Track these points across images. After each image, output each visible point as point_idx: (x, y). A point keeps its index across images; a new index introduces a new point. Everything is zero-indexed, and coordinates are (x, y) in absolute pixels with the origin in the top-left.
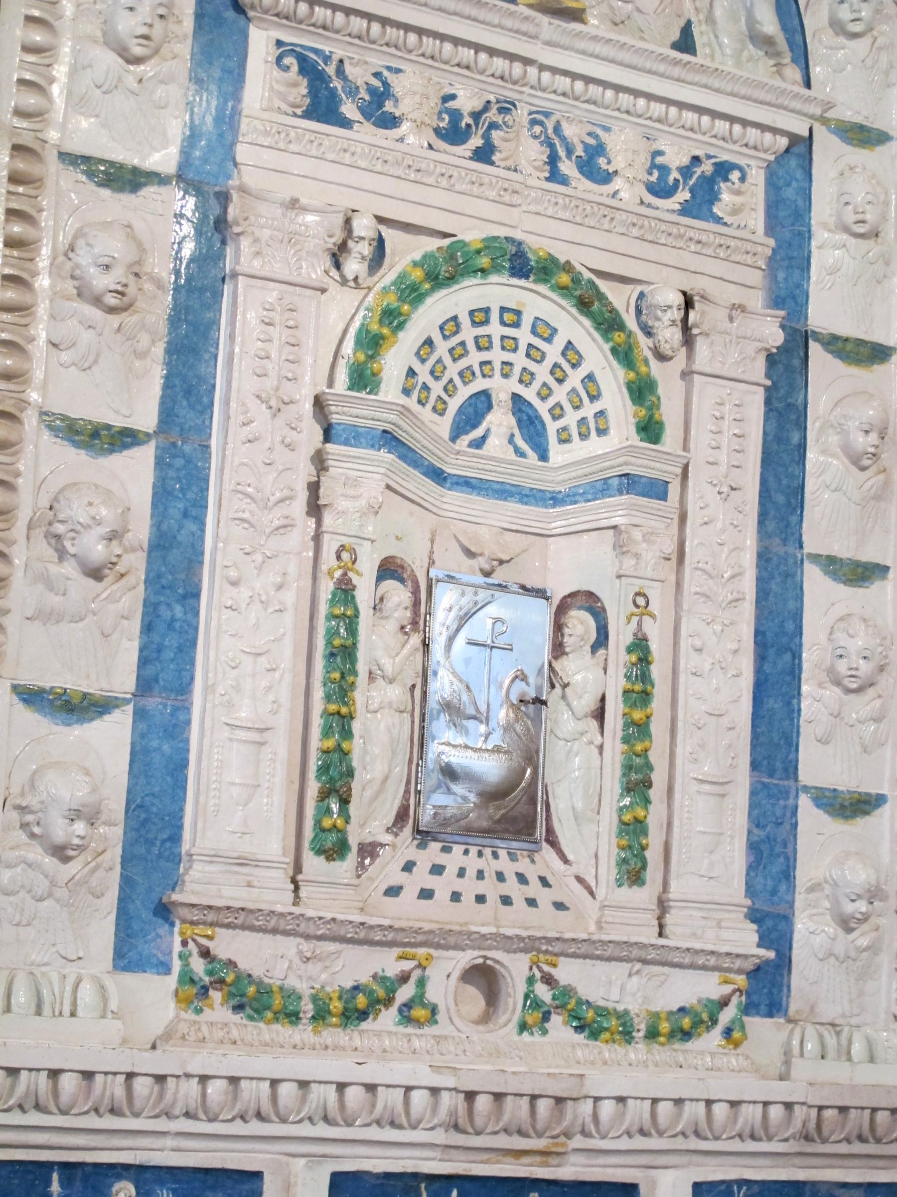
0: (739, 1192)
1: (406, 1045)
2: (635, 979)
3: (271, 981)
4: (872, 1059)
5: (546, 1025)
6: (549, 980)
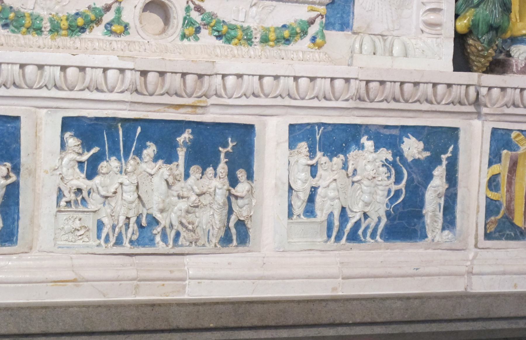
0: (319, 130)
1: (108, 46)
2: (254, 9)
3: (25, 11)
4: (406, 55)
5: (198, 35)
6: (199, 9)
